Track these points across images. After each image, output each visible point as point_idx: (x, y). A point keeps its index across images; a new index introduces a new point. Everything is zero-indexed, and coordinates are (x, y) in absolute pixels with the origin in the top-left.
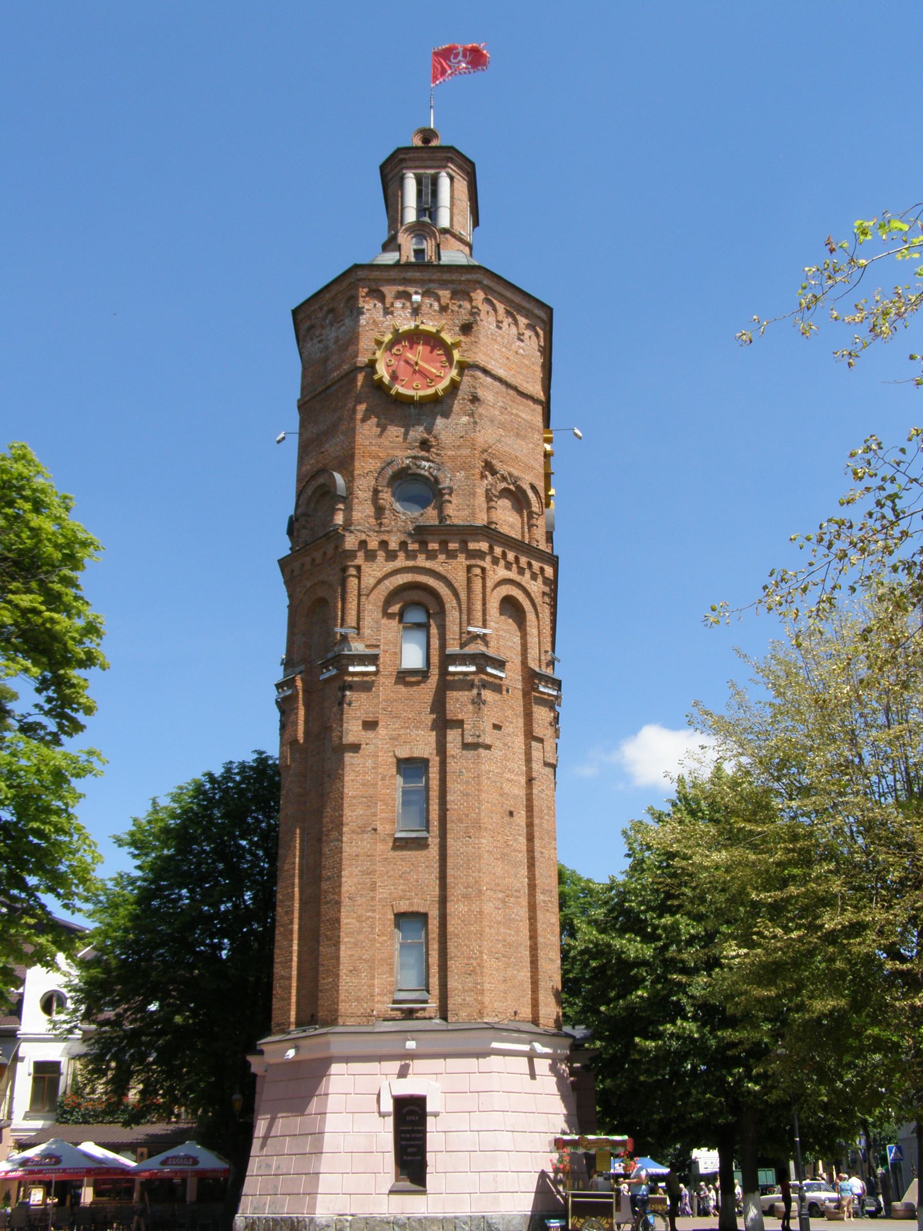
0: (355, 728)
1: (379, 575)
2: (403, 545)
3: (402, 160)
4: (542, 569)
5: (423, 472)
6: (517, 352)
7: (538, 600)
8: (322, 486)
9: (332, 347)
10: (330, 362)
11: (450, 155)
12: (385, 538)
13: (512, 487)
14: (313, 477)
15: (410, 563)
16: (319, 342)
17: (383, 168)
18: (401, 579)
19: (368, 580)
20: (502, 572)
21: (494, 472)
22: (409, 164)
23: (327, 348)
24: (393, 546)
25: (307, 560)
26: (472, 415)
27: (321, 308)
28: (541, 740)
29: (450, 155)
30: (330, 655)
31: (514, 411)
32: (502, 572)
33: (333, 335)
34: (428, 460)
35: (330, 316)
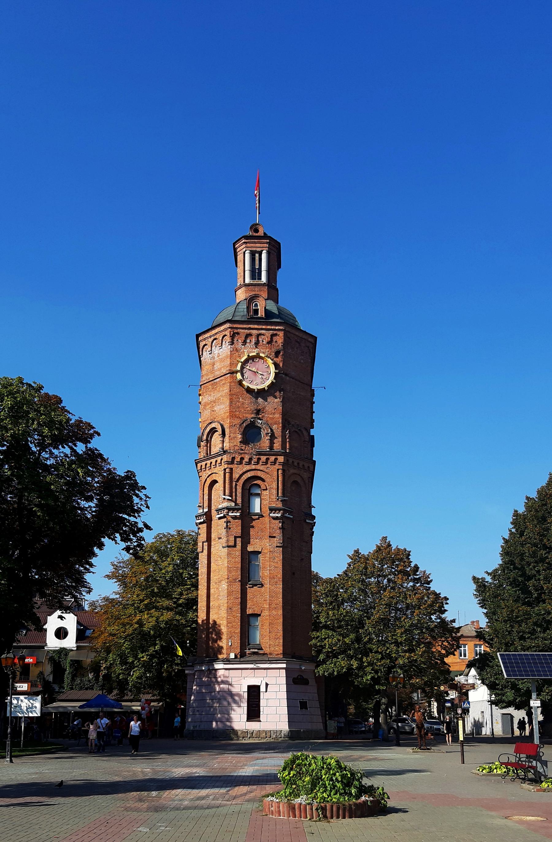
0: (231, 539)
1: (241, 473)
2: (251, 459)
3: (244, 242)
4: (308, 467)
5: (259, 425)
6: (300, 362)
7: (307, 481)
8: (215, 428)
9: (216, 358)
10: (215, 366)
11: (268, 241)
12: (243, 456)
13: (296, 430)
14: (211, 423)
15: (254, 467)
16: (210, 354)
17: (234, 244)
18: (249, 475)
19: (236, 476)
20: (292, 471)
21: (289, 423)
22: (248, 245)
23: (214, 358)
24: (246, 459)
25: (209, 462)
26: (280, 399)
27: (210, 337)
28: (307, 543)
29: (268, 241)
30: (220, 507)
31: (298, 393)
32: (292, 471)
33: (216, 352)
34: (261, 420)
35: (215, 342)
